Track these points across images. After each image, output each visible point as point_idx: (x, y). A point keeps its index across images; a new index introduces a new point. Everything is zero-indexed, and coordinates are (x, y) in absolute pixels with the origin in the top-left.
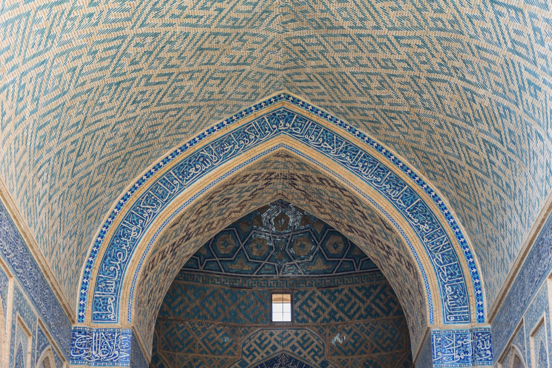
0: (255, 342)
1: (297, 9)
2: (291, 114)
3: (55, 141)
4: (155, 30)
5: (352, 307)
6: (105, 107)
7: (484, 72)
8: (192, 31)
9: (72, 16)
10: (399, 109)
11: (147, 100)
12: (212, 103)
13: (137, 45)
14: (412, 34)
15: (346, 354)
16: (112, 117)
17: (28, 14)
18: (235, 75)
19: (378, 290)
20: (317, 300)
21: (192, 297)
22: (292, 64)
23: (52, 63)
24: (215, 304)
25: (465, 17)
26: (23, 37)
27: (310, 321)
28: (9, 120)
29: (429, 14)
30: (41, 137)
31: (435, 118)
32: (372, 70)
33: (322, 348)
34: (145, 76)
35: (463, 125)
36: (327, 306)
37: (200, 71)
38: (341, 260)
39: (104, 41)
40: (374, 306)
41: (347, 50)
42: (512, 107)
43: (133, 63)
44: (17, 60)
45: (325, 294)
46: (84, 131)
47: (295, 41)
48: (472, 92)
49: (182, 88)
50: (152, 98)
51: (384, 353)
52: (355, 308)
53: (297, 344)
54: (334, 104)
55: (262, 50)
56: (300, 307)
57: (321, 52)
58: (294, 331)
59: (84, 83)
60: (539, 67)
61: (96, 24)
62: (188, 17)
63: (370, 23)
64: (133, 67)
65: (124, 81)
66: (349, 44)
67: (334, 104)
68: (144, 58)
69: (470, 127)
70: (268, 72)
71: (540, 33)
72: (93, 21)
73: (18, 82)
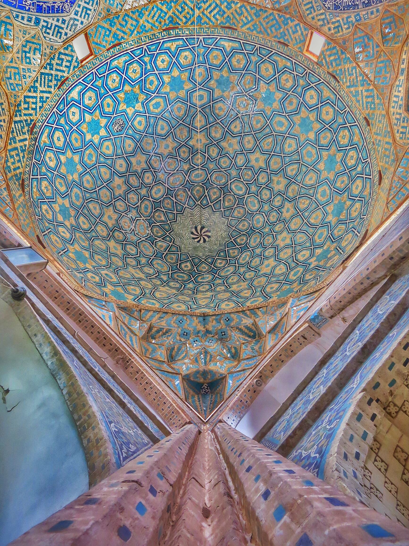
0: (90, 10)
5: (44, 83)
15: (27, 41)
19: (38, 108)
20: (64, 69)
21: (146, 24)
24: (129, 26)
27: (62, 51)
33: (45, 35)
36: (57, 70)
38: (66, 108)
40: (34, 95)
45: (61, 77)
51: (6, 64)
52: (43, 82)
53: (63, 26)
56: (72, 56)
58: (69, 35)
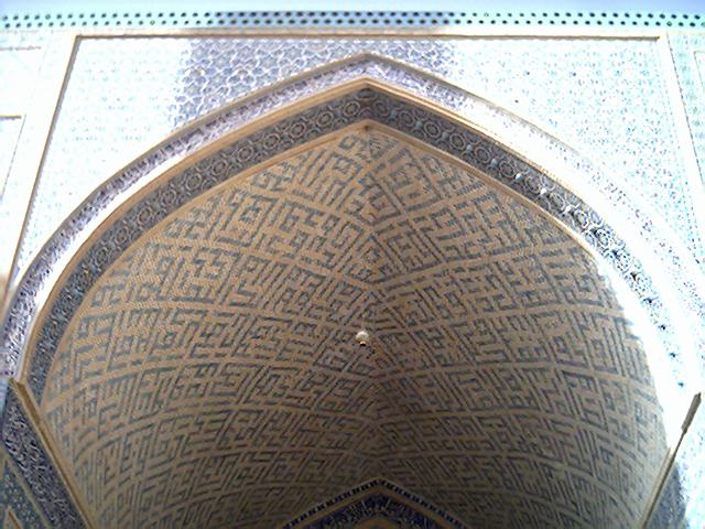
1: (390, 395)
2: (386, 499)
3: (160, 507)
4: (260, 407)
6: (212, 478)
7: (559, 445)
8: (294, 411)
9: (179, 384)
10: (485, 490)
11: (251, 477)
12: (313, 484)
13: (241, 420)
14: (492, 413)
16: (219, 489)
17: (135, 376)
18: (335, 457)
22: (386, 450)
23: (159, 428)
25: (541, 393)
26: (130, 398)
28: (113, 476)
29: (508, 392)
30: (147, 500)
31: (516, 496)
32: (458, 453)
34: (249, 453)
35: (542, 501)
37: (301, 452)
39: (210, 414)
41: (435, 434)
42: (587, 477)
43: (237, 438)
44: (124, 419)
46: (191, 501)
47: (388, 428)
48: (550, 468)
49: (284, 467)
50: (257, 475)
54: (425, 488)
55: (358, 436)
57: (412, 437)
59: (190, 453)
60: (611, 433)
61: (202, 396)
62: (289, 397)
63: (456, 405)
64: (238, 443)
65: (229, 455)
66: (437, 427)
67: (425, 488)
68: (250, 434)
69: (549, 503)
70: (365, 458)
71: (610, 398)
72: (200, 391)
73: (123, 440)
